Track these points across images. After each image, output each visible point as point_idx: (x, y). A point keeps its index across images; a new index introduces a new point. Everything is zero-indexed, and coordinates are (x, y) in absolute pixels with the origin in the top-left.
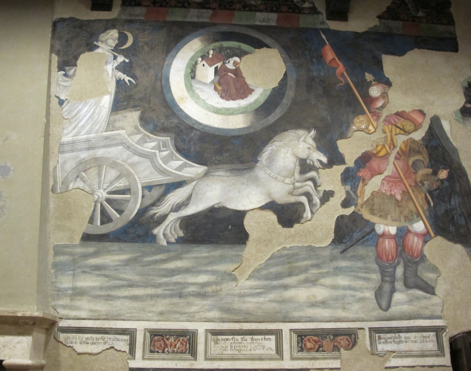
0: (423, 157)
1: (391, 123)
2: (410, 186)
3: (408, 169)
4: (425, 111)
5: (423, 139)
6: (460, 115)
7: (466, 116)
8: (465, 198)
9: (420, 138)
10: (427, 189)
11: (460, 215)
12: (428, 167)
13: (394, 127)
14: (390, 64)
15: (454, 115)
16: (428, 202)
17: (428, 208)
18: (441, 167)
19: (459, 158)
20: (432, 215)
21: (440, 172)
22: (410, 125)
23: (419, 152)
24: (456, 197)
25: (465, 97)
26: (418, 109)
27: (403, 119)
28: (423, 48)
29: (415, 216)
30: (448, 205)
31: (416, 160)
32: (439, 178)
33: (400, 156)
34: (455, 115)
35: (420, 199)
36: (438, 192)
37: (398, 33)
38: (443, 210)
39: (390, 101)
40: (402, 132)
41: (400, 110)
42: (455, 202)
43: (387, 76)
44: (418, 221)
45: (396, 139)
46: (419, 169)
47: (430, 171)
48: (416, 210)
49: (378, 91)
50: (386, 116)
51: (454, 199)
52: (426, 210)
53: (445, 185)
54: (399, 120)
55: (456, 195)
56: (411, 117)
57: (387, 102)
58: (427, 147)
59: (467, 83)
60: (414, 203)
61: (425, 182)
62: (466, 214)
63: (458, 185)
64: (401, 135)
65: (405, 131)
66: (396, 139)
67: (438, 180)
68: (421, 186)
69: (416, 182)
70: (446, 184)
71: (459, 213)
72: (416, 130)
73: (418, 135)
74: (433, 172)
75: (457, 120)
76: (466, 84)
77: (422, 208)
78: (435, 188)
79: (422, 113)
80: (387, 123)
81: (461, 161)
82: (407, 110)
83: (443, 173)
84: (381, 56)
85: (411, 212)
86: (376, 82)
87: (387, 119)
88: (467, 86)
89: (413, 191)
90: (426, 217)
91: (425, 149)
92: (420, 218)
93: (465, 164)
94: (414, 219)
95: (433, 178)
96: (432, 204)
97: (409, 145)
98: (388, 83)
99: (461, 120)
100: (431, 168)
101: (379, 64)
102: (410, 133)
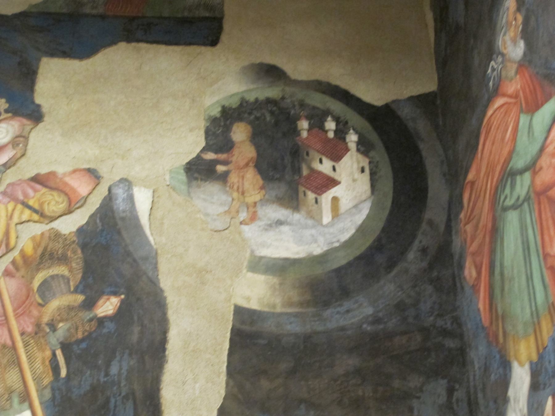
0: (69, 271)
1: (16, 200)
2: (22, 334)
3: (28, 297)
4: (103, 170)
5: (81, 231)
6: (183, 177)
7: (196, 179)
8: (146, 358)
9: (74, 229)
10: (61, 339)
11: (126, 397)
12: (76, 291)
13: (20, 206)
14: (55, 78)
15: (167, 177)
16: (56, 369)
17: (52, 382)
18: (108, 290)
19: (155, 267)
20: (58, 396)
21: (101, 302)
22: (57, 202)
23: (63, 259)
24: (126, 356)
25: (206, 138)
26: (87, 166)
27: (44, 190)
28: (138, 41)
29: (16, 400)
30: (103, 374)
31: (53, 277)
32: (96, 316)
33: (17, 269)
34: (172, 178)
35: (38, 364)
36: (84, 345)
37: (94, 12)
38: (86, 387)
39: (29, 152)
40: (36, 217)
41: (44, 170)
42: (121, 369)
43: (38, 100)
44: (21, 411)
45: (17, 231)
46: (54, 296)
47: (80, 298)
48: (22, 388)
49: (8, 132)
50: (9, 185)
51: (120, 361)
52: (46, 387)
53: (105, 331)
54: (35, 191)
55: (127, 351)
56: (66, 184)
57: (19, 155)
58: (84, 247)
59: (220, 109)
60: (21, 371)
61: (61, 325)
62: (139, 394)
63: (136, 329)
64: (31, 224)
65: (42, 215)
66: (17, 231)
67: (91, 320)
68: (48, 333)
69: (38, 325)
70: (110, 326)
71: (123, 394)
72: (69, 211)
73: (69, 225)
74: (84, 301)
75: (174, 189)
76: (216, 112)
77: (37, 380)
78: (80, 335)
79: (93, 174)
80: (6, 200)
81: (160, 277)
82: (60, 170)
83: (108, 303)
84: (39, 60)
85: (10, 392)
86: (10, 115)
87: (9, 190)
88: (218, 115)
89: (26, 345)
90: (41, 403)
91: (79, 251)
92: (26, 404)
93: (166, 283)
94: (11, 406)
95: (80, 314)
96: (64, 373)
97: (43, 245)
98: (36, 116)
99: (184, 187)
100: (82, 292)
101: (29, 75)
102: (53, 219)
